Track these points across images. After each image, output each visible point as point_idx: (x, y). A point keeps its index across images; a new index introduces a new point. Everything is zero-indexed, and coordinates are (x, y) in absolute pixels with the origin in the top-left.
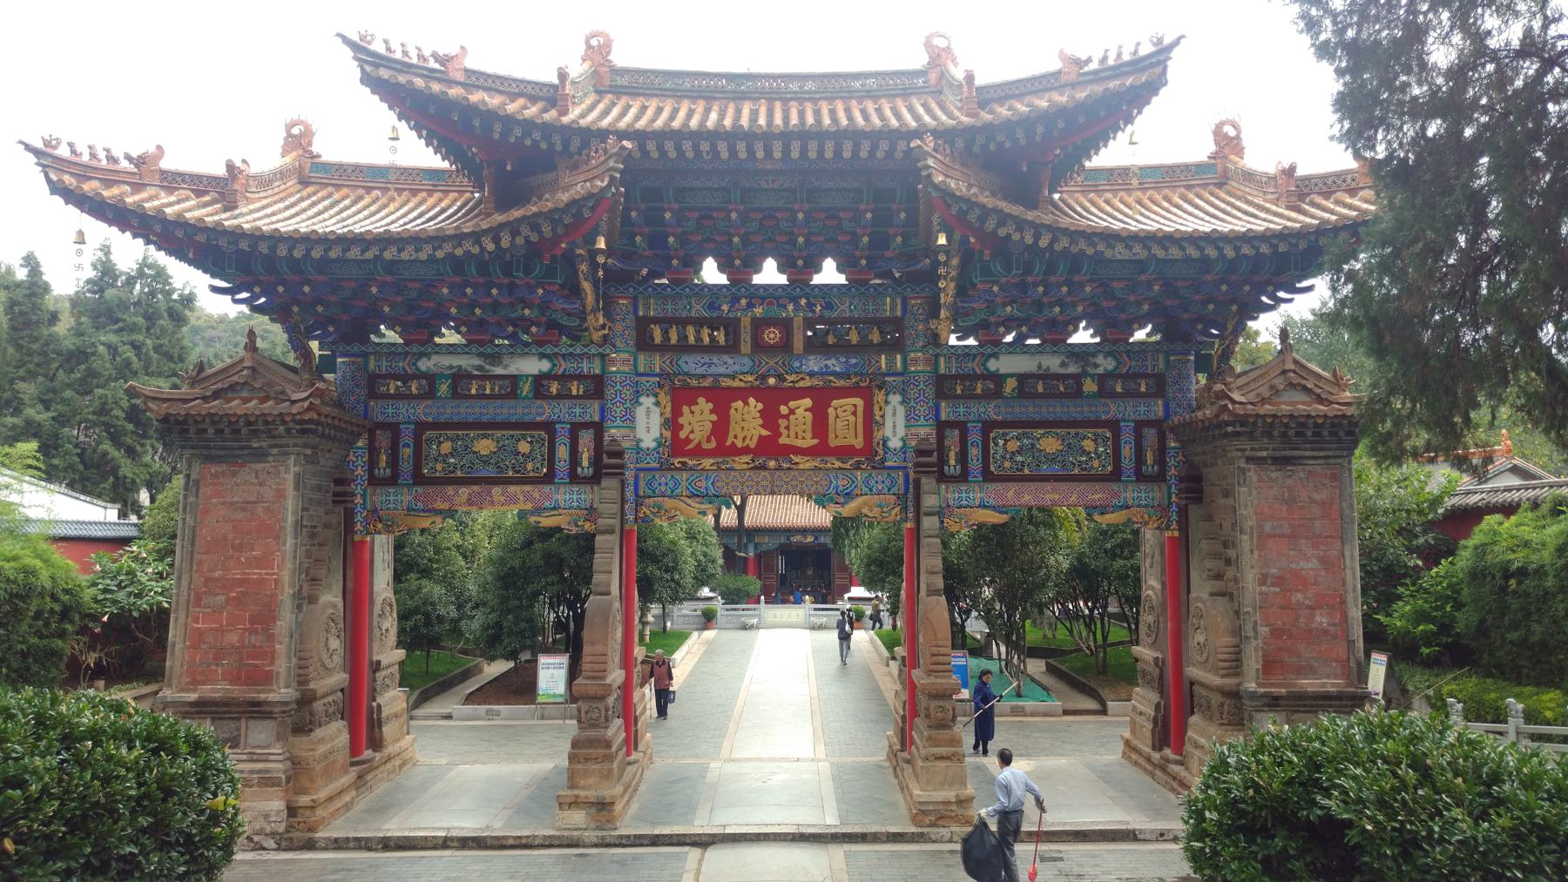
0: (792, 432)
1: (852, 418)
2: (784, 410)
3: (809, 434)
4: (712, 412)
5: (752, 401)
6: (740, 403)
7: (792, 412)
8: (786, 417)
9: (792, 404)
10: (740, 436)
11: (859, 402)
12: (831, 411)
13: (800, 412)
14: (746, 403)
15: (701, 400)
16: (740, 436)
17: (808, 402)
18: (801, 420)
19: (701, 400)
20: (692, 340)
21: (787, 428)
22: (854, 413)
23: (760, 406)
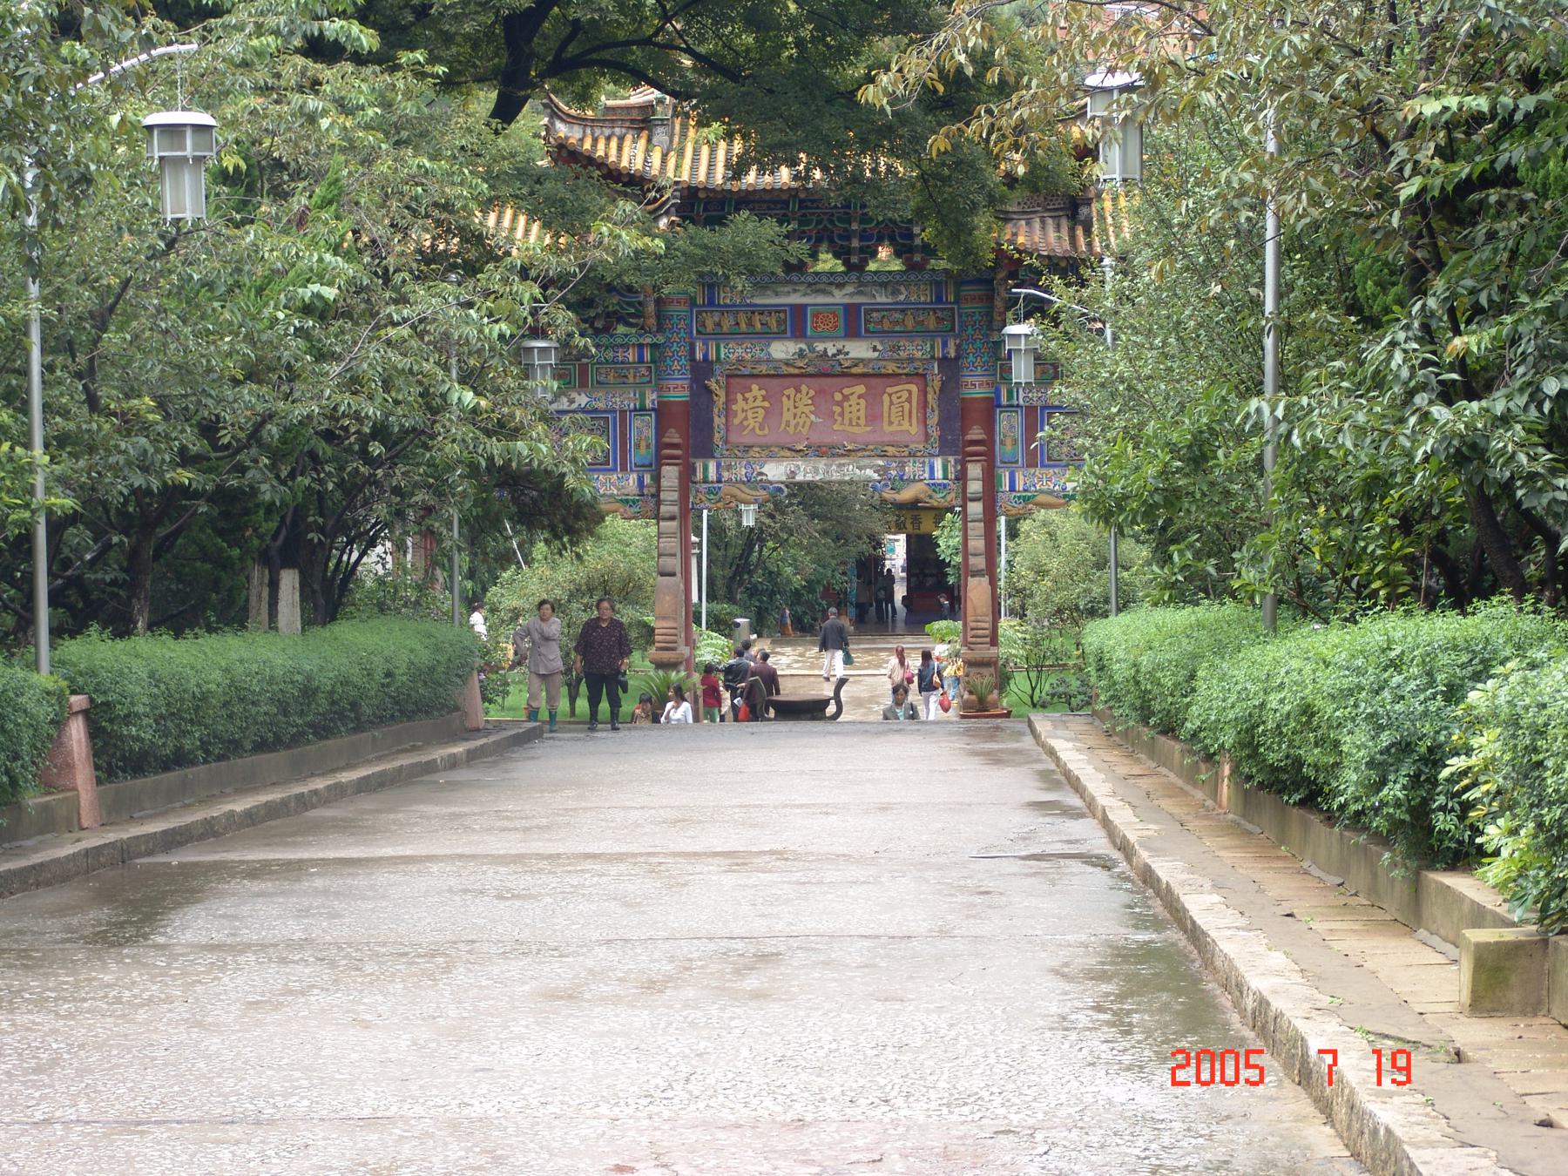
0: (846, 421)
1: (906, 405)
2: (838, 397)
3: (863, 421)
4: (764, 399)
5: (804, 388)
6: (791, 391)
7: (846, 398)
8: (840, 404)
9: (846, 391)
10: (793, 422)
11: (914, 388)
12: (886, 397)
13: (853, 399)
14: (798, 390)
15: (755, 387)
16: (793, 422)
17: (861, 389)
18: (854, 409)
19: (755, 387)
20: (743, 327)
21: (842, 414)
22: (909, 400)
23: (812, 393)
